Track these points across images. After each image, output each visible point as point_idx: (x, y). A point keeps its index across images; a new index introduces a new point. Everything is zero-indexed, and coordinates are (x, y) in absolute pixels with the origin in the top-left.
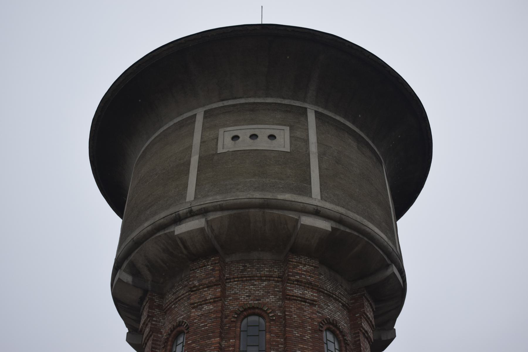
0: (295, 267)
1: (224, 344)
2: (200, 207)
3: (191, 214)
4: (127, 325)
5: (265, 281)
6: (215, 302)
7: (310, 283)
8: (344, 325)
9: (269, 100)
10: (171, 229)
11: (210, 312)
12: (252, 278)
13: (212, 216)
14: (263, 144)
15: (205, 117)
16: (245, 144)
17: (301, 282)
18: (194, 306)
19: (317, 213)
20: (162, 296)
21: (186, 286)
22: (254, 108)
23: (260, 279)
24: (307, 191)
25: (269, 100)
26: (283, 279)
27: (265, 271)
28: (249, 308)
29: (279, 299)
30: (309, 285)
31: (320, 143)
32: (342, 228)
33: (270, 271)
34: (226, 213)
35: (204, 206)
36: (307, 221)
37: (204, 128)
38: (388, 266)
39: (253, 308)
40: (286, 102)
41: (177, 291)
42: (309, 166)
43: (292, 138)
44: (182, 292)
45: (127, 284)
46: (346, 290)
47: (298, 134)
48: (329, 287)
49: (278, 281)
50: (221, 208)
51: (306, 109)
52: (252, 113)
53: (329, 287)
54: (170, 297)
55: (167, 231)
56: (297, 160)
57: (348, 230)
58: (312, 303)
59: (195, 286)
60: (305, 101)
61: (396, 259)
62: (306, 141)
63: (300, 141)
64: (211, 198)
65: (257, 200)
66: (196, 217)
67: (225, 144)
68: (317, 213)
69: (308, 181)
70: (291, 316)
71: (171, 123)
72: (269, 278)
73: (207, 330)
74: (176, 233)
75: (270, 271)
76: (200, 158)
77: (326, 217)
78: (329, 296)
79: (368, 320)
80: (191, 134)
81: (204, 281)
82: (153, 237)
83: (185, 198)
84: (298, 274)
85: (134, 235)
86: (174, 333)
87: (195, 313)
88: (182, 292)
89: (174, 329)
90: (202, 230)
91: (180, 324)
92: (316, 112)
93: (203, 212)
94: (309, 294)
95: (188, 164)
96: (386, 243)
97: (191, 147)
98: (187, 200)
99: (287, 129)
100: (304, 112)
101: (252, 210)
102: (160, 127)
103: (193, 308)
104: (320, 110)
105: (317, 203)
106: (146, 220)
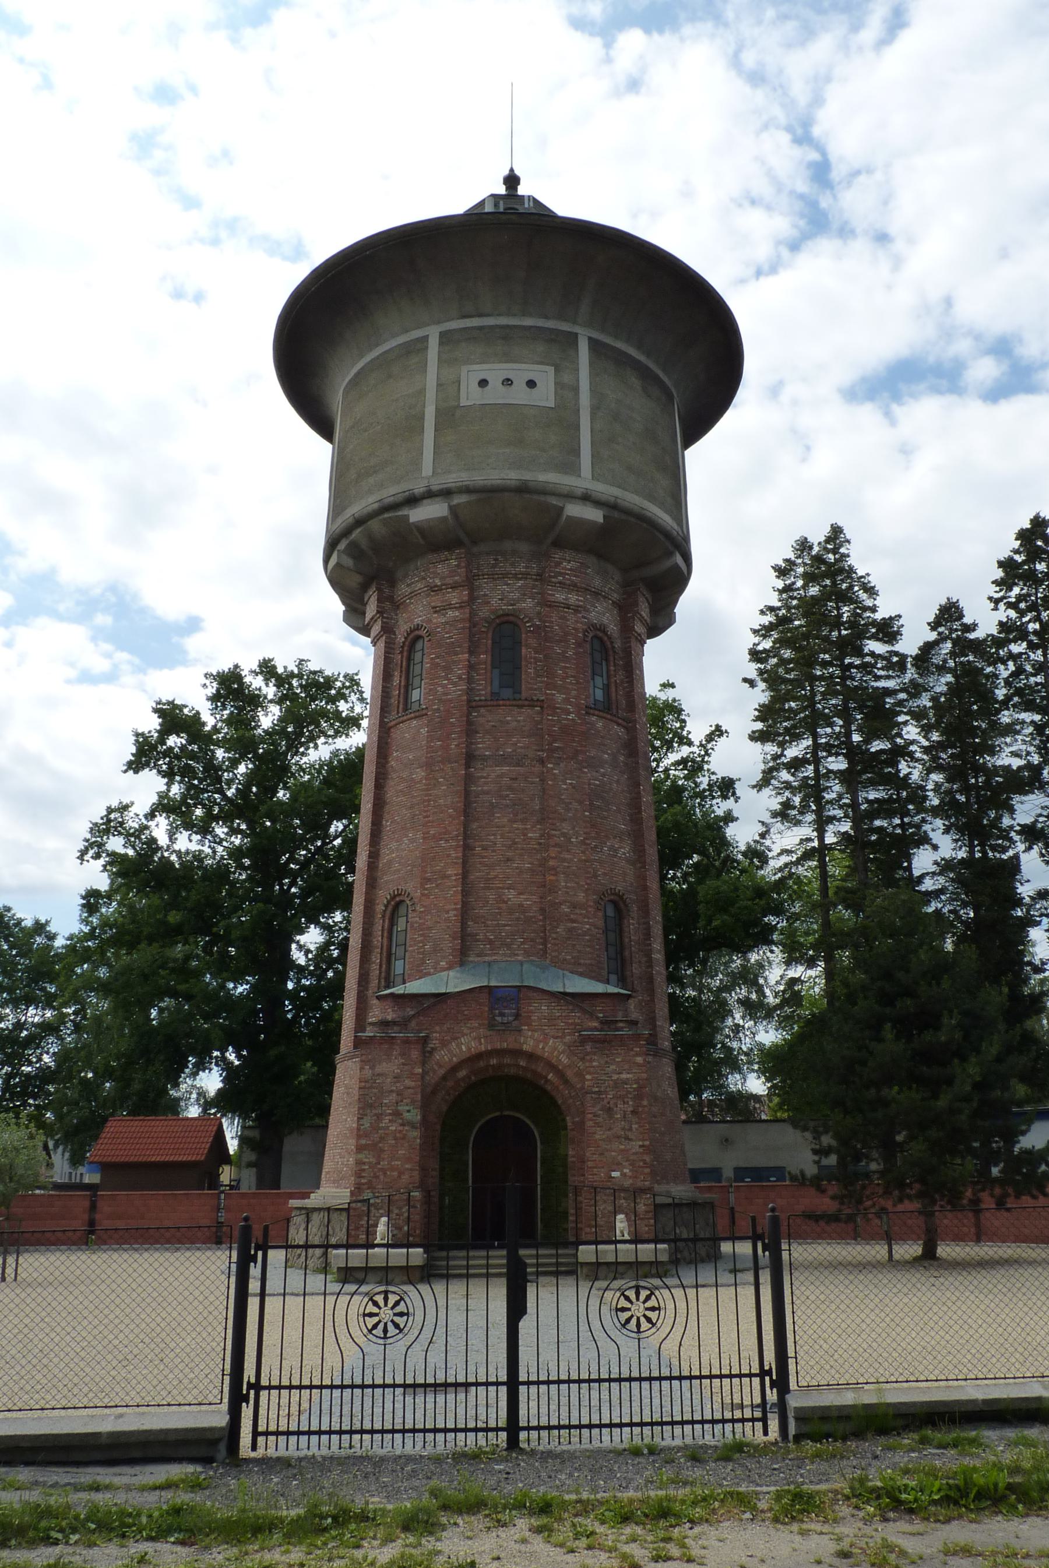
0: (558, 564)
1: (473, 660)
2: (441, 487)
3: (430, 495)
4: (344, 603)
5: (520, 579)
6: (461, 607)
7: (575, 585)
8: (613, 629)
9: (528, 322)
11: (456, 620)
12: (505, 575)
13: (457, 500)
14: (519, 395)
15: (441, 344)
16: (496, 394)
17: (564, 584)
18: (436, 610)
19: (586, 498)
20: (393, 583)
21: (424, 578)
22: (506, 334)
23: (515, 577)
25: (528, 322)
26: (540, 577)
27: (521, 568)
28: (503, 615)
29: (538, 604)
30: (574, 587)
31: (593, 391)
32: (616, 514)
33: (527, 567)
34: (473, 497)
35: (445, 486)
36: (574, 510)
38: (670, 554)
39: (508, 615)
40: (550, 324)
42: (577, 427)
43: (559, 385)
44: (419, 585)
45: (349, 569)
46: (617, 582)
47: (566, 378)
48: (597, 582)
49: (536, 580)
50: (467, 490)
51: (576, 334)
52: (503, 341)
53: (597, 582)
54: (403, 589)
55: (400, 513)
56: (562, 417)
57: (624, 517)
58: (577, 610)
59: (436, 586)
60: (575, 323)
61: (680, 545)
62: (576, 389)
63: (567, 390)
64: (454, 475)
65: (513, 482)
66: (437, 499)
67: (470, 395)
68: (586, 498)
69: (576, 452)
70: (552, 627)
72: (525, 576)
73: (453, 643)
74: (412, 520)
75: (527, 567)
77: (598, 503)
78: (596, 594)
79: (642, 619)
80: (423, 368)
82: (381, 517)
83: (420, 470)
84: (561, 574)
85: (356, 509)
86: (411, 636)
87: (438, 619)
88: (419, 585)
89: (411, 631)
90: (443, 519)
91: (418, 628)
92: (590, 338)
93: (446, 493)
94: (573, 598)
95: (422, 418)
96: (669, 528)
97: (422, 392)
98: (424, 474)
99: (551, 370)
100: (572, 339)
101: (506, 494)
102: (377, 345)
103: (435, 612)
104: (595, 335)
105: (587, 482)
106: (370, 492)
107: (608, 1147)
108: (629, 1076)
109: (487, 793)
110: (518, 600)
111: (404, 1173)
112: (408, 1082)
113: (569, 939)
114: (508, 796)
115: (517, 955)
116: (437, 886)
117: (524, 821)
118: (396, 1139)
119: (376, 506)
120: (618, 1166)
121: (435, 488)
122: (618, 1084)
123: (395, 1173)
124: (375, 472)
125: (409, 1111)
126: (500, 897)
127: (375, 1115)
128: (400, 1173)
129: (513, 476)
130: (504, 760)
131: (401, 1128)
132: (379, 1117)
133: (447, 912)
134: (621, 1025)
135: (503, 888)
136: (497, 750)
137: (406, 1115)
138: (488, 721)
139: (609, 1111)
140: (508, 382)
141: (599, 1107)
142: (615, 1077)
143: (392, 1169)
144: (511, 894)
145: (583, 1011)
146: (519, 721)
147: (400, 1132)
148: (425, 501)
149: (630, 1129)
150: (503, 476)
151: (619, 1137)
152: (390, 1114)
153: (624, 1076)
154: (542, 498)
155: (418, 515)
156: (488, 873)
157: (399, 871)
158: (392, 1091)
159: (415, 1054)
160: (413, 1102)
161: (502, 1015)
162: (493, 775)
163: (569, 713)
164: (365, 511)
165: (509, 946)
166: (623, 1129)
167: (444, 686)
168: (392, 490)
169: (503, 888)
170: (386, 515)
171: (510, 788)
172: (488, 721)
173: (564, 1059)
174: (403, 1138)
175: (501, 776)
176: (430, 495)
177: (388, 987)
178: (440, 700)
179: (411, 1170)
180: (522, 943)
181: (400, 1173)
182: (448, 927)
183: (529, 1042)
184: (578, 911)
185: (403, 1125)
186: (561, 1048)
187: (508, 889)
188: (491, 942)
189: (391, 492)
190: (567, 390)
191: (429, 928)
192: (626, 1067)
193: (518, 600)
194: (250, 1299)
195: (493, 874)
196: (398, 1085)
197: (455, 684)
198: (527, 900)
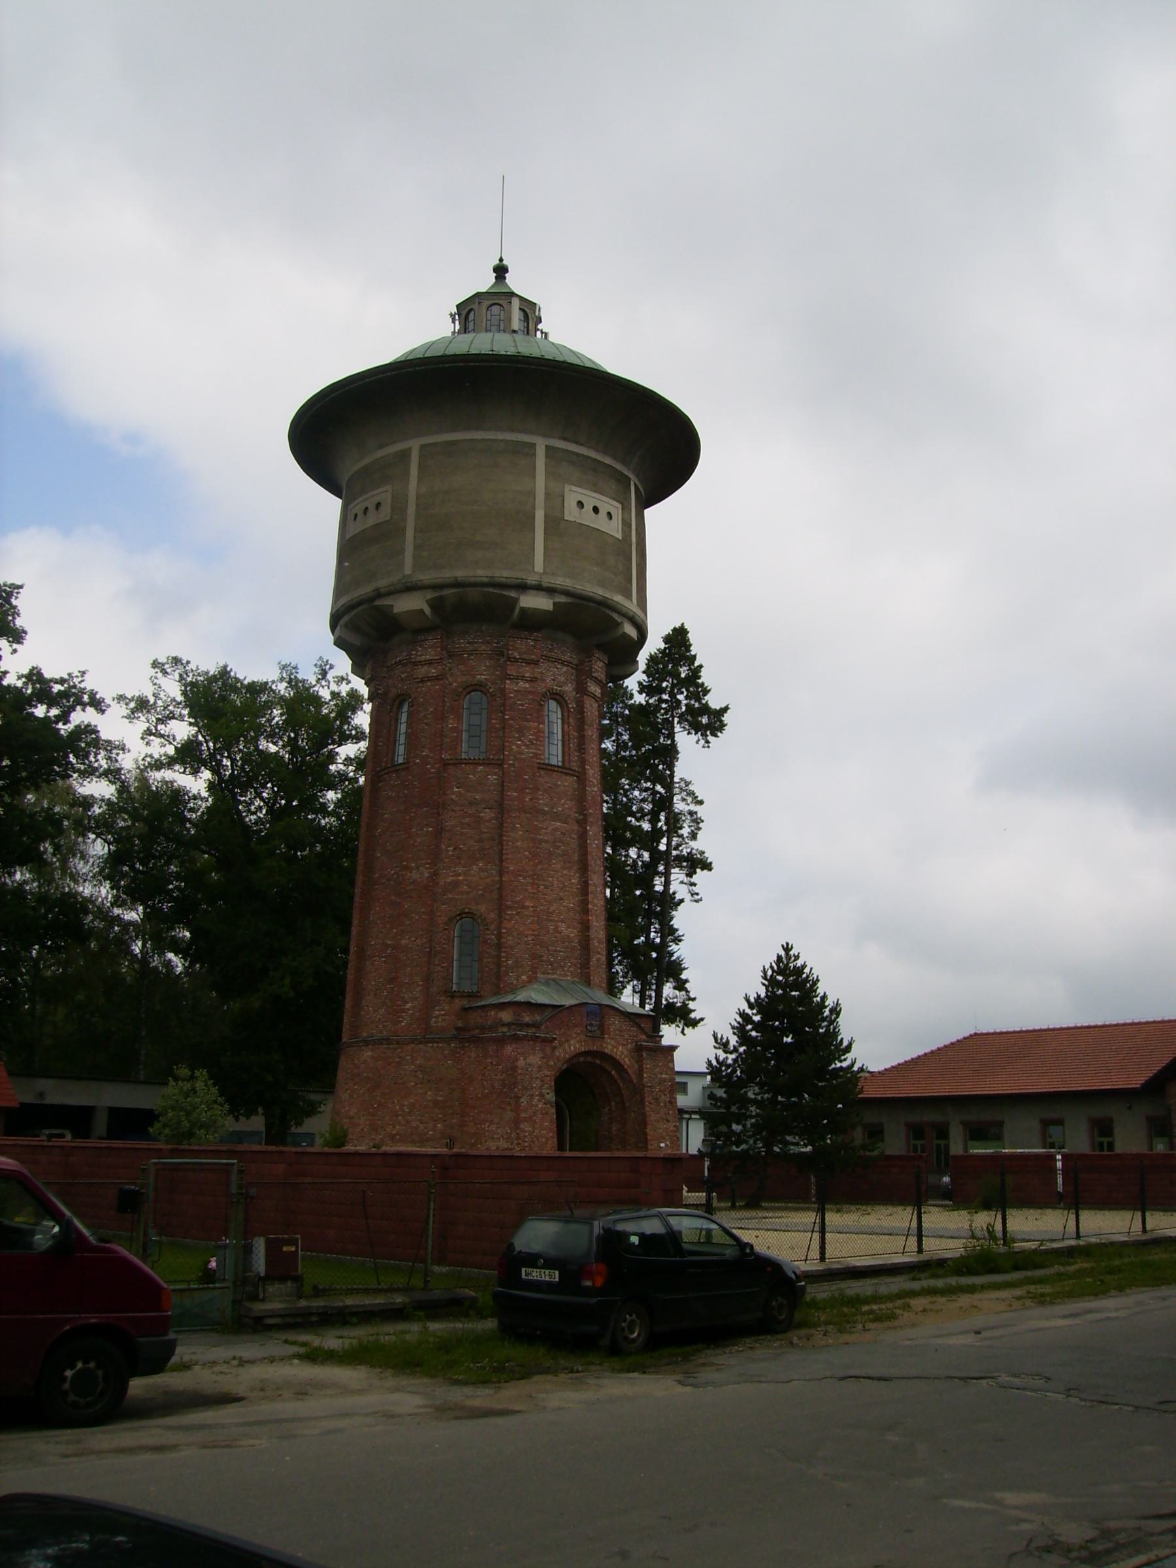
3: (538, 588)
12: (557, 660)
23: (563, 663)
27: (567, 658)
34: (569, 600)
37: (548, 474)
44: (484, 647)
50: (567, 593)
71: (500, 436)
81: (525, 656)
93: (551, 591)
97: (532, 494)
102: (478, 428)
109: (546, 842)
116: (518, 913)
117: (570, 868)
119: (486, 580)
121: (545, 585)
128: (547, 1140)
129: (600, 592)
137: (548, 1097)
139: (657, 1099)
140: (596, 510)
144: (563, 927)
145: (639, 1026)
148: (533, 592)
154: (607, 611)
157: (468, 893)
159: (548, 1050)
161: (591, 1025)
162: (550, 829)
164: (473, 580)
165: (562, 967)
167: (519, 746)
168: (506, 573)
170: (491, 590)
171: (561, 841)
176: (538, 588)
177: (497, 992)
178: (516, 759)
181: (547, 1140)
186: (625, 1052)
189: (504, 574)
191: (512, 948)
194: (901, 1217)
197: (528, 747)
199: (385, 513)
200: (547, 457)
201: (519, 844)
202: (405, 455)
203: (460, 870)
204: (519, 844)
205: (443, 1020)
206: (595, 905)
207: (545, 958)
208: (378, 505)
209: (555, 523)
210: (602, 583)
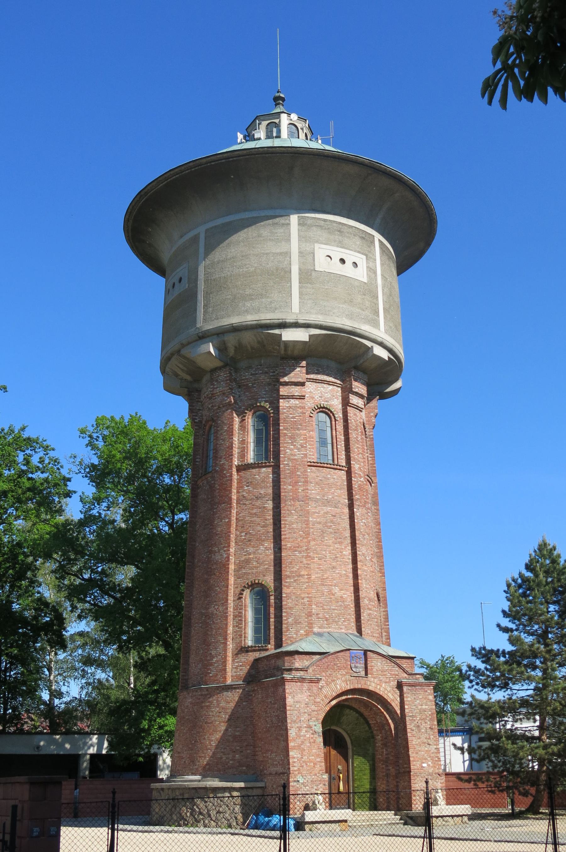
3: (296, 325)
10: (277, 331)
14: (347, 270)
16: (336, 268)
21: (267, 373)
24: (376, 324)
37: (301, 238)
41: (257, 374)
44: (263, 376)
47: (371, 264)
62: (375, 273)
64: (314, 316)
68: (381, 344)
69: (377, 313)
74: (284, 338)
76: (300, 270)
90: (304, 343)
93: (307, 326)
97: (287, 254)
107: (420, 749)
108: (427, 707)
109: (320, 523)
110: (330, 399)
111: (316, 764)
112: (313, 707)
113: (368, 620)
114: (331, 526)
115: (341, 629)
116: (295, 581)
117: (341, 543)
118: (310, 743)
120: (424, 760)
121: (301, 321)
122: (422, 711)
123: (312, 764)
124: (252, 299)
125: (315, 725)
126: (330, 591)
127: (298, 727)
130: (328, 503)
131: (312, 736)
132: (300, 729)
133: (303, 599)
134: (418, 676)
135: (331, 585)
136: (324, 496)
137: (314, 727)
138: (318, 476)
141: (413, 725)
142: (420, 707)
143: (311, 762)
144: (336, 590)
146: (334, 478)
147: (312, 738)
149: (429, 739)
150: (343, 323)
151: (425, 743)
152: (306, 727)
153: (424, 707)
155: (289, 335)
156: (323, 575)
158: (305, 713)
159: (315, 689)
160: (317, 720)
161: (356, 667)
162: (322, 512)
163: (361, 477)
166: (426, 738)
169: (331, 585)
171: (332, 522)
172: (318, 476)
173: (390, 695)
174: (314, 742)
175: (327, 513)
176: (296, 325)
179: (320, 762)
180: (344, 621)
182: (304, 608)
183: (372, 684)
184: (371, 603)
185: (312, 734)
186: (389, 689)
187: (335, 586)
188: (327, 620)
190: (372, 271)
191: (291, 608)
192: (425, 701)
193: (330, 399)
195: (326, 576)
196: (308, 708)
197: (298, 449)
198: (344, 594)
199: (185, 285)
200: (299, 224)
201: (294, 526)
202: (196, 239)
203: (251, 550)
204: (294, 526)
205: (241, 670)
206: (364, 571)
207: (320, 616)
208: (180, 280)
209: (307, 276)
210: (350, 316)
